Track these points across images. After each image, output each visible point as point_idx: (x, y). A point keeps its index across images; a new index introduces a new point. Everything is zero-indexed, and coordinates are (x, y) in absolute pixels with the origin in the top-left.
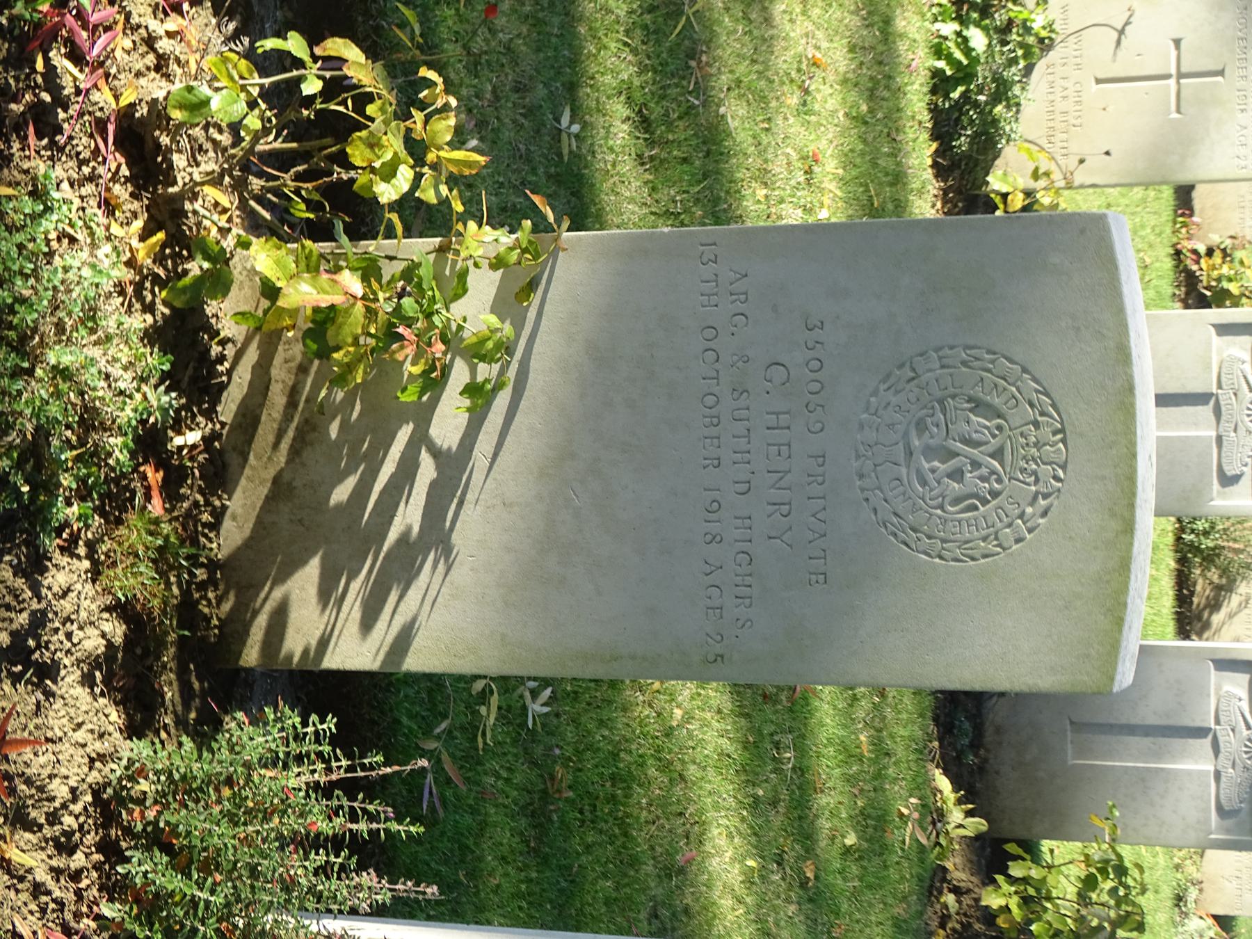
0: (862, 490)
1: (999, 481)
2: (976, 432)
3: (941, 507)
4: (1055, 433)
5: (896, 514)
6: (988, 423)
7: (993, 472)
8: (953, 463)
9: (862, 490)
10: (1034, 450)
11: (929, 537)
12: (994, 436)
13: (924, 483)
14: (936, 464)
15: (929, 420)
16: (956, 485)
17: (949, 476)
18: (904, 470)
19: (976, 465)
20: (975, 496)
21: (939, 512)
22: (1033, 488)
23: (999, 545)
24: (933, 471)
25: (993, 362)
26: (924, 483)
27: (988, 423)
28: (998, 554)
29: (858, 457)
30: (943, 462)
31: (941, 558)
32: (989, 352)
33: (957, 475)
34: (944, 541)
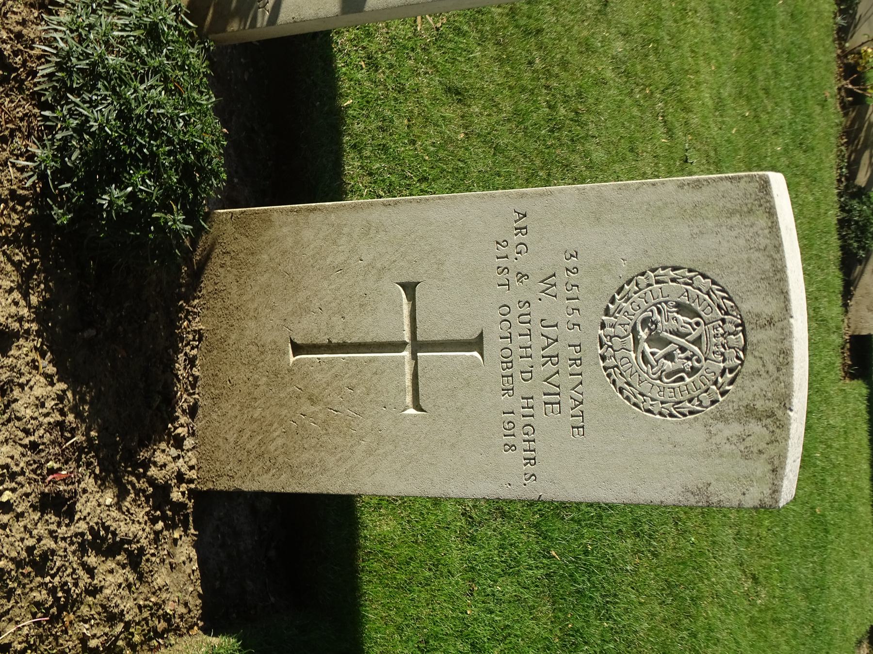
0: (606, 369)
1: (698, 361)
3: (660, 379)
7: (694, 355)
9: (606, 369)
12: (694, 330)
13: (646, 361)
16: (669, 363)
18: (633, 355)
19: (683, 349)
20: (683, 371)
21: (658, 382)
22: (722, 365)
24: (653, 354)
26: (646, 361)
33: (669, 357)
34: (662, 403)
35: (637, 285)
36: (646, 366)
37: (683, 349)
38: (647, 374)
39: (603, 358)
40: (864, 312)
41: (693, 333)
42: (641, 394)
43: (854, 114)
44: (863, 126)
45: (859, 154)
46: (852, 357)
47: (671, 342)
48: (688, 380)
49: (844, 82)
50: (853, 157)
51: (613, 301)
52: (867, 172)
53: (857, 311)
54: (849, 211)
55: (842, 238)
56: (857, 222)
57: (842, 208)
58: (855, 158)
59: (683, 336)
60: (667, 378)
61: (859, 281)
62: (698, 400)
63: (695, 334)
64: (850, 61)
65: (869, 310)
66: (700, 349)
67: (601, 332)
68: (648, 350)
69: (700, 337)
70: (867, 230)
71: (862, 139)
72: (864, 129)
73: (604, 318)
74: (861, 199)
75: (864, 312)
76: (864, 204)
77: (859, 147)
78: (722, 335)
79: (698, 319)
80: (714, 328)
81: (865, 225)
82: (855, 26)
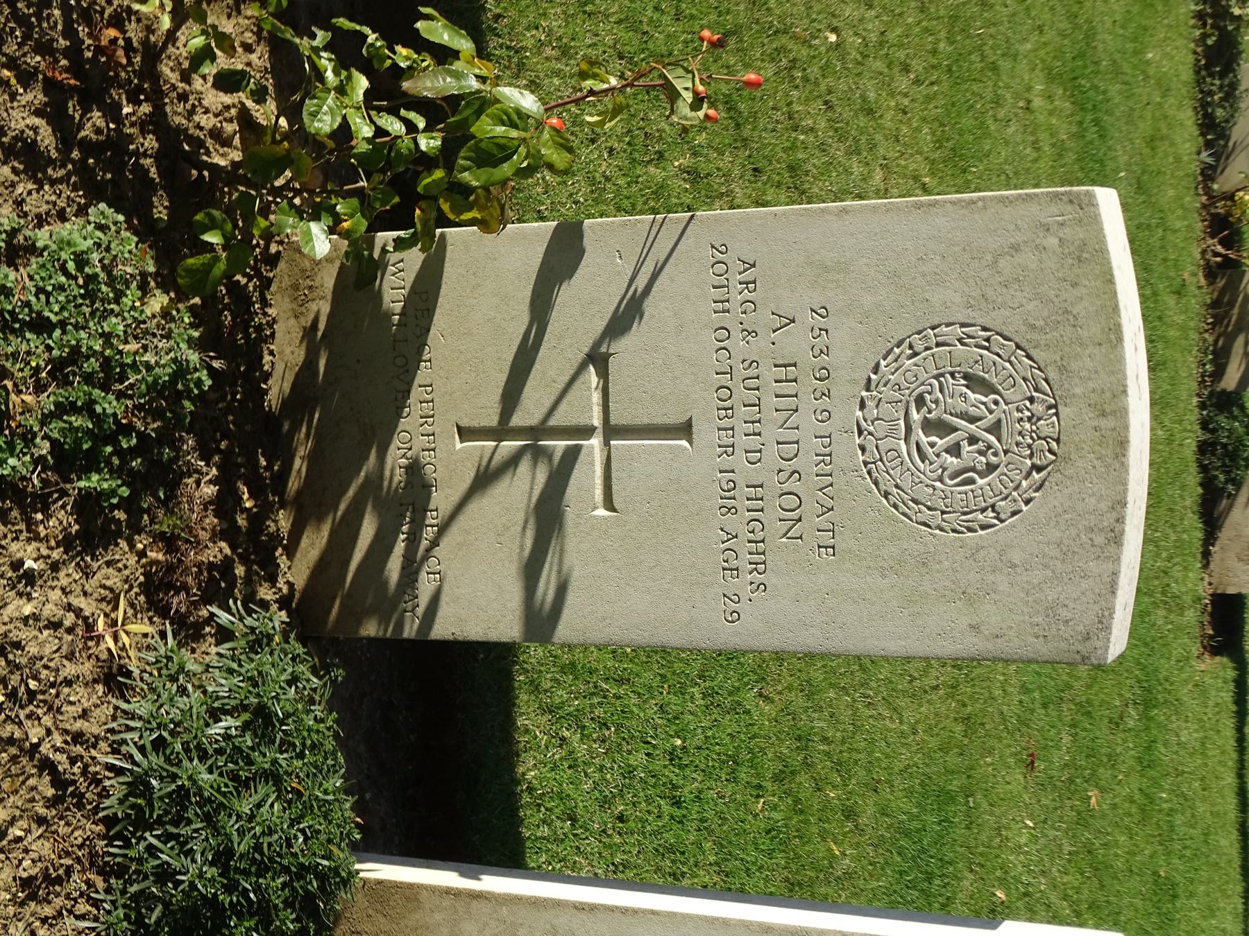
1: (995, 454)
2: (973, 405)
3: (941, 480)
4: (1050, 407)
5: (897, 486)
6: (984, 399)
7: (989, 447)
8: (950, 439)
9: (866, 463)
10: (1027, 426)
11: (929, 509)
12: (991, 412)
13: (923, 457)
14: (934, 439)
15: (928, 397)
16: (954, 459)
17: (947, 451)
19: (973, 440)
20: (973, 469)
21: (938, 484)
23: (997, 518)
24: (932, 445)
25: (988, 340)
26: (923, 457)
27: (984, 399)
28: (993, 526)
29: (860, 433)
30: (941, 439)
31: (942, 530)
32: (985, 329)
33: (955, 450)
34: (943, 512)
35: (911, 347)
36: (923, 462)
37: (973, 440)
38: (924, 474)
39: (863, 449)
40: (1233, 563)
41: (990, 417)
42: (913, 500)
43: (1223, 282)
44: (1236, 300)
45: (1231, 339)
46: (1213, 624)
47: (956, 430)
48: (980, 482)
49: (1210, 242)
50: (1220, 343)
51: (876, 370)
52: (1240, 365)
53: (1222, 560)
54: (1213, 431)
55: (1203, 468)
56: (1224, 446)
57: (1204, 424)
58: (1223, 345)
59: (973, 420)
60: (952, 479)
61: (1226, 518)
62: (993, 511)
63: (991, 418)
64: (1220, 211)
65: (1240, 560)
66: (999, 440)
67: (859, 413)
68: (924, 440)
69: (999, 421)
70: (1239, 456)
71: (1234, 318)
72: (1238, 305)
73: (864, 393)
74: (1231, 413)
75: (1233, 563)
76: (1235, 418)
77: (1230, 328)
78: (1029, 419)
79: (997, 397)
80: (1018, 410)
81: (1236, 450)
82: (1227, 158)
